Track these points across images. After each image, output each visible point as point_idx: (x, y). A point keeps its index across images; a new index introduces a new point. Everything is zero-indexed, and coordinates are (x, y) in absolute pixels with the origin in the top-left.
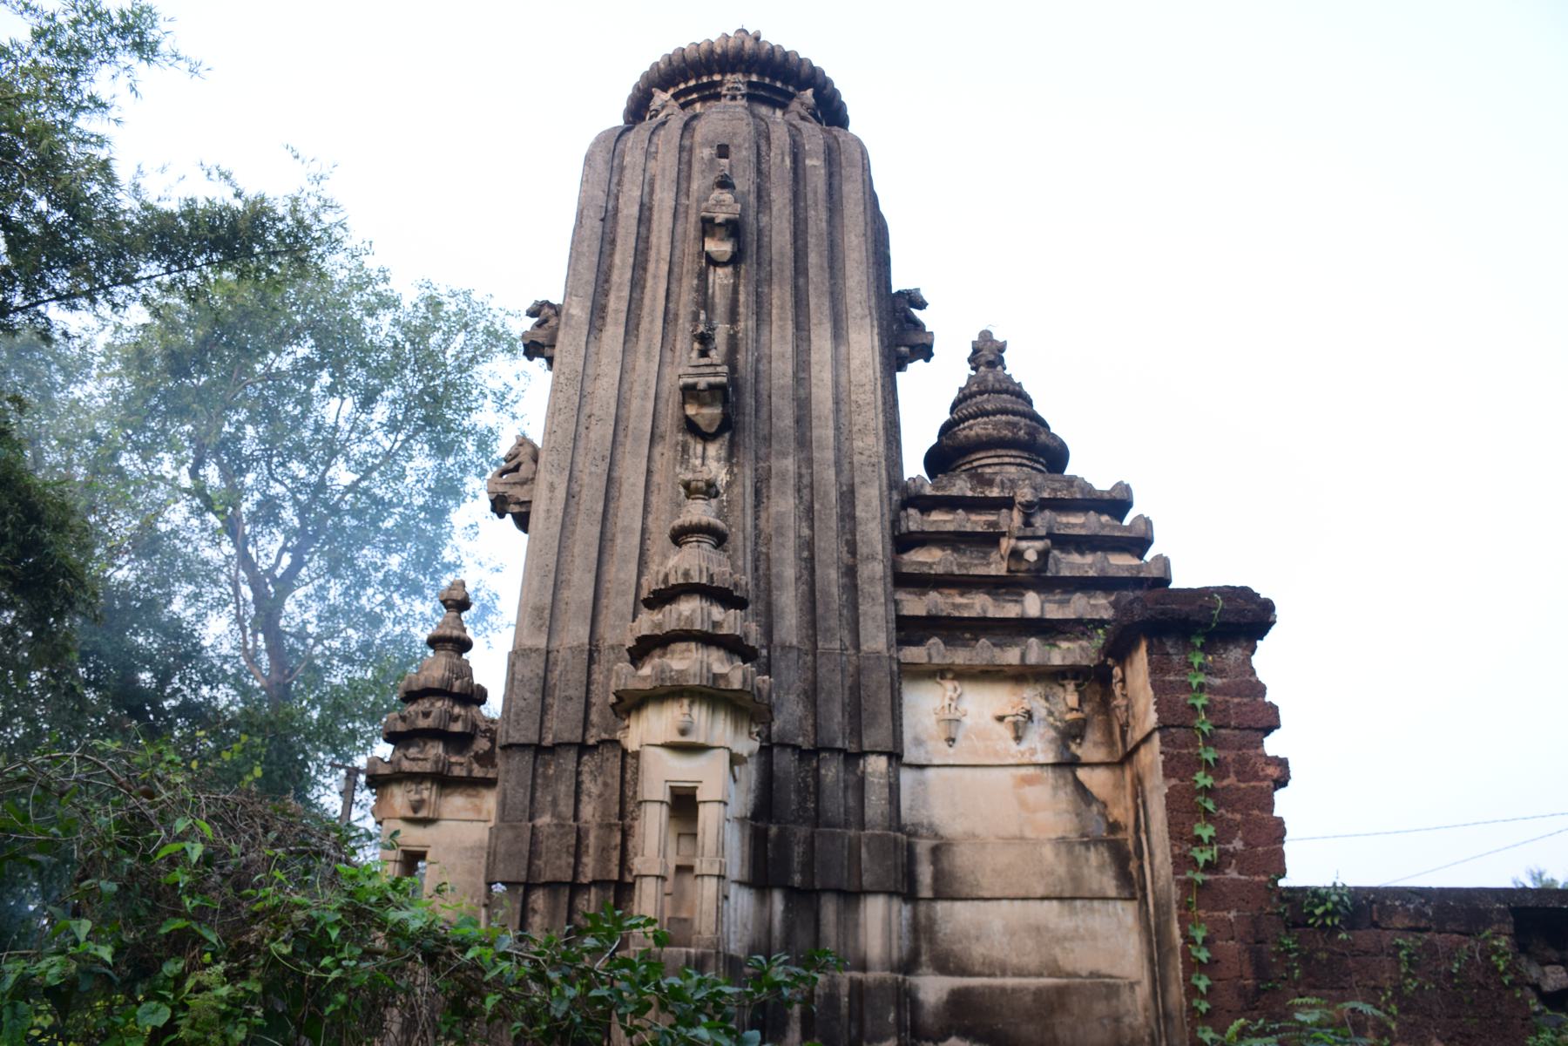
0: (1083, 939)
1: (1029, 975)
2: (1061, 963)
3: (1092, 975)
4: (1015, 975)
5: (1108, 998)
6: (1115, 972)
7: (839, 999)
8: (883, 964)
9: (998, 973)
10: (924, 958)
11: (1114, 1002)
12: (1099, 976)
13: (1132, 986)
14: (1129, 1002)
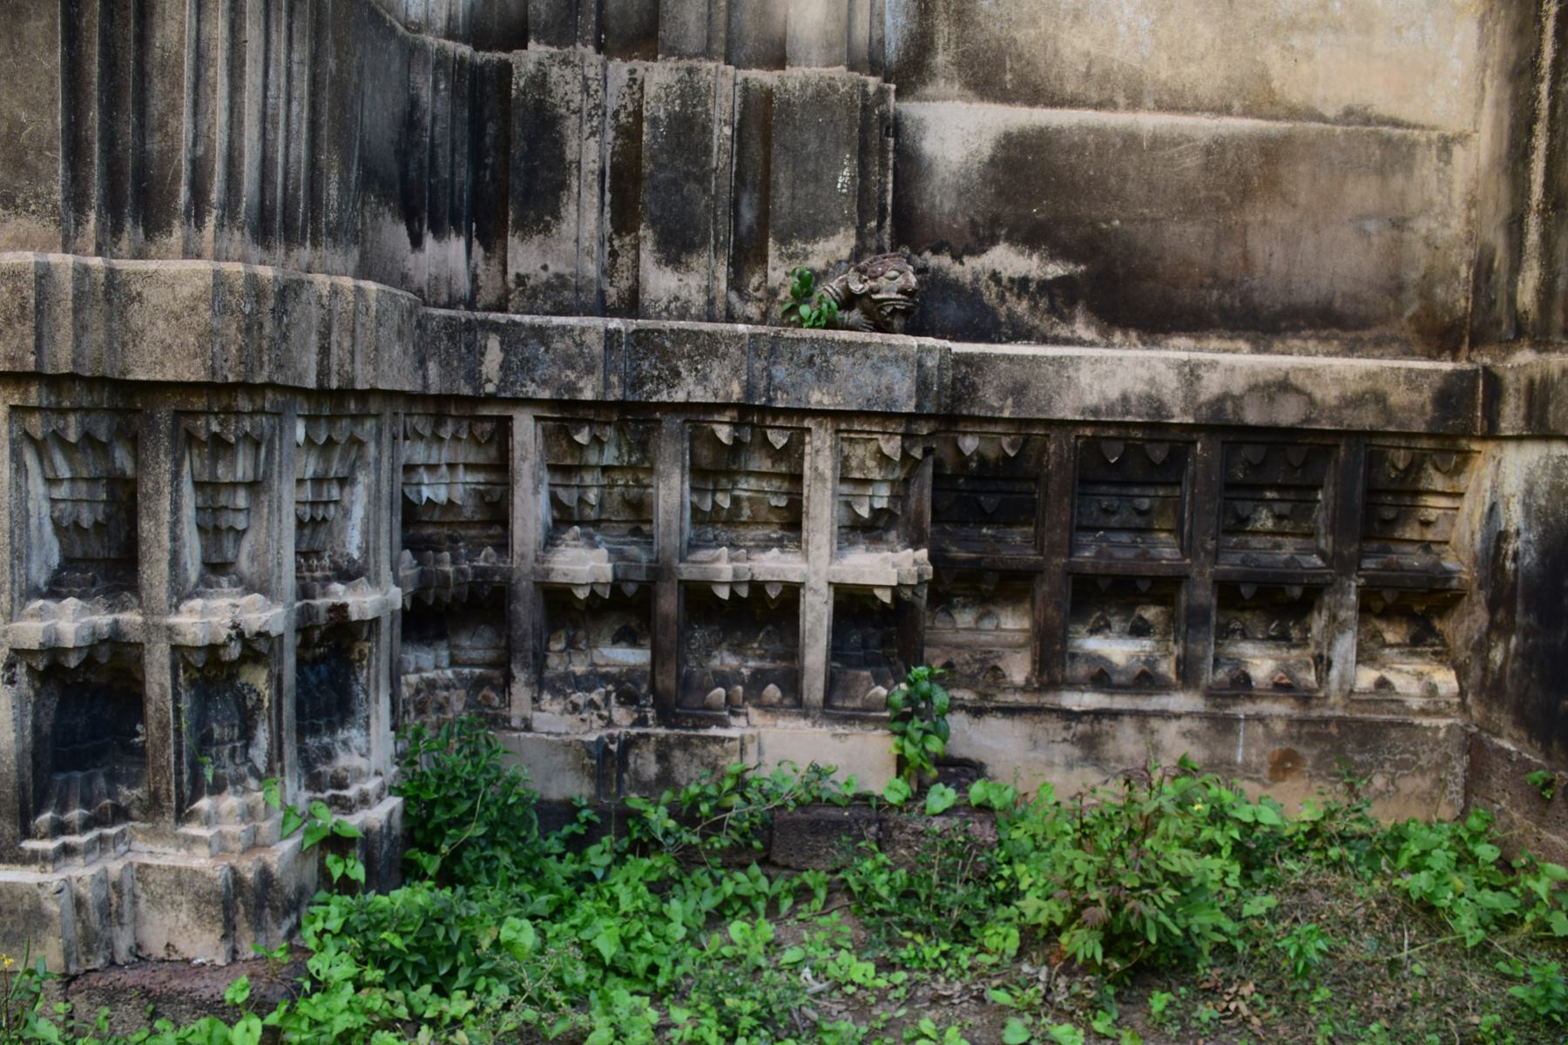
0: (1338, 28)
1: (1197, 108)
2: (1276, 84)
3: (1349, 115)
4: (1160, 107)
5: (1382, 171)
6: (1407, 113)
7: (706, 130)
8: (830, 46)
9: (1121, 99)
10: (941, 59)
11: (1397, 182)
12: (1367, 121)
13: (1446, 145)
14: (1433, 183)
